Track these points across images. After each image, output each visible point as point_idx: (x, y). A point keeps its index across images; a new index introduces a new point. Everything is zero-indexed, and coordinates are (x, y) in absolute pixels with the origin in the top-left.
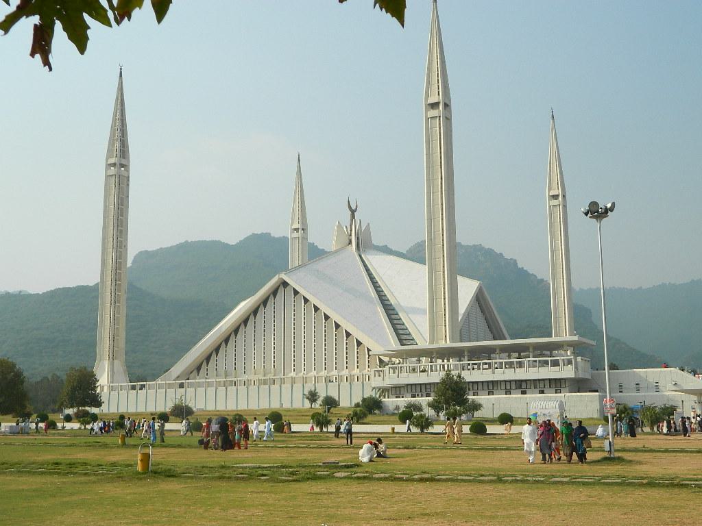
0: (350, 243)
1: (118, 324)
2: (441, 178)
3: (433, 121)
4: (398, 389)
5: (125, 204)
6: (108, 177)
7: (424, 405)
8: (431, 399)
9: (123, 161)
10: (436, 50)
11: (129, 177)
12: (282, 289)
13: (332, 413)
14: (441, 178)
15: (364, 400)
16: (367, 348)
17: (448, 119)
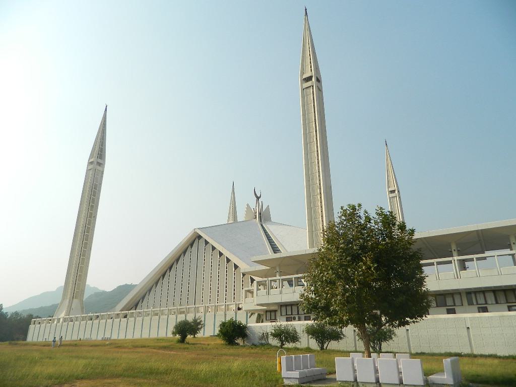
0: (256, 218)
1: (82, 272)
2: (316, 131)
3: (308, 90)
4: (273, 314)
5: (97, 189)
6: (88, 170)
7: (298, 330)
8: (310, 322)
9: (100, 161)
10: (308, 40)
11: (103, 171)
12: (197, 240)
13: (188, 343)
14: (316, 131)
15: (223, 325)
16: (219, 252)
17: (320, 90)
